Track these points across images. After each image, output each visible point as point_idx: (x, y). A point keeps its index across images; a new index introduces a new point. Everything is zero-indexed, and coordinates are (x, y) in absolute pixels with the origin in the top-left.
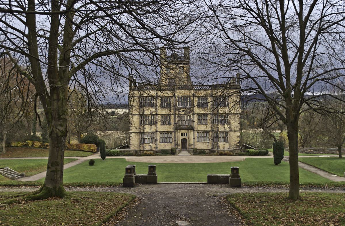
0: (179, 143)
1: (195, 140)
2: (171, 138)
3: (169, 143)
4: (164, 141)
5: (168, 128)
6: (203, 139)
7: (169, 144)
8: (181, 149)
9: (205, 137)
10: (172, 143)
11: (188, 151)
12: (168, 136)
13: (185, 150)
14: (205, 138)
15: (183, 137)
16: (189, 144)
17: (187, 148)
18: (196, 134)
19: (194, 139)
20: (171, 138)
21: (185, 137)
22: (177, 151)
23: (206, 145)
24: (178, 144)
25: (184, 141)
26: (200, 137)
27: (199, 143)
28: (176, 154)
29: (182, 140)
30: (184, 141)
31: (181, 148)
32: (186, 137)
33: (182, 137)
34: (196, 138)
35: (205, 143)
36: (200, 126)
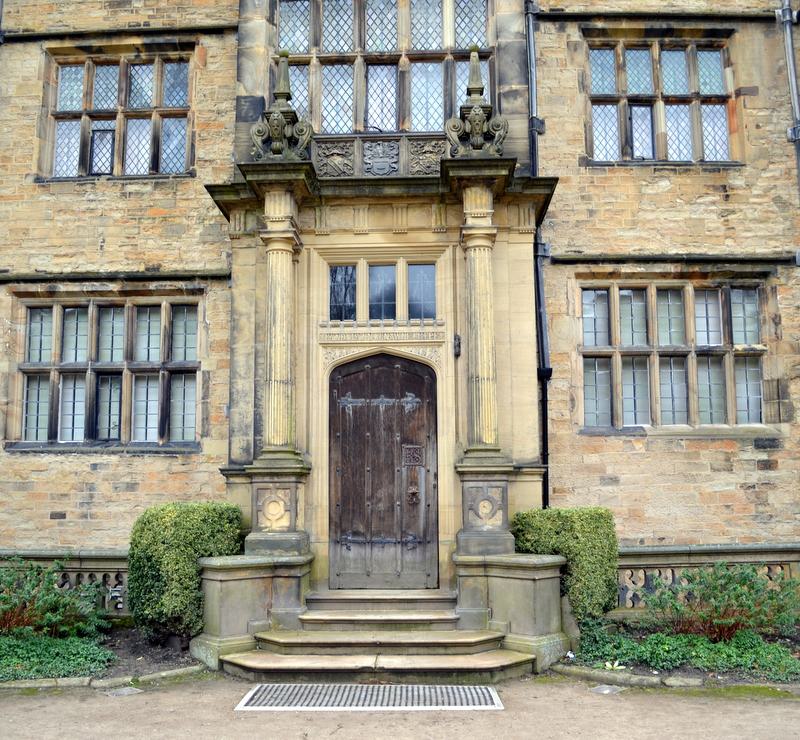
0: (275, 434)
1: (555, 385)
2: (188, 372)
3: (144, 450)
4: (74, 428)
5: (136, 216)
6: (663, 382)
7: (157, 465)
8: (322, 546)
9: (705, 355)
10: (192, 449)
11: (448, 586)
12: (151, 351)
13: (388, 555)
14: (702, 378)
15: (364, 336)
16: (472, 446)
17: (428, 537)
18: (576, 323)
19: (544, 375)
20: (188, 372)
21: (400, 337)
22: (234, 610)
23: (727, 483)
24: (257, 449)
25: (383, 399)
26: (636, 360)
27: (613, 453)
28: (206, 651)
29: (346, 377)
30: (383, 399)
31: (320, 525)
32: (417, 329)
33: (344, 330)
34: (569, 371)
35: (708, 455)
36: (623, 187)
